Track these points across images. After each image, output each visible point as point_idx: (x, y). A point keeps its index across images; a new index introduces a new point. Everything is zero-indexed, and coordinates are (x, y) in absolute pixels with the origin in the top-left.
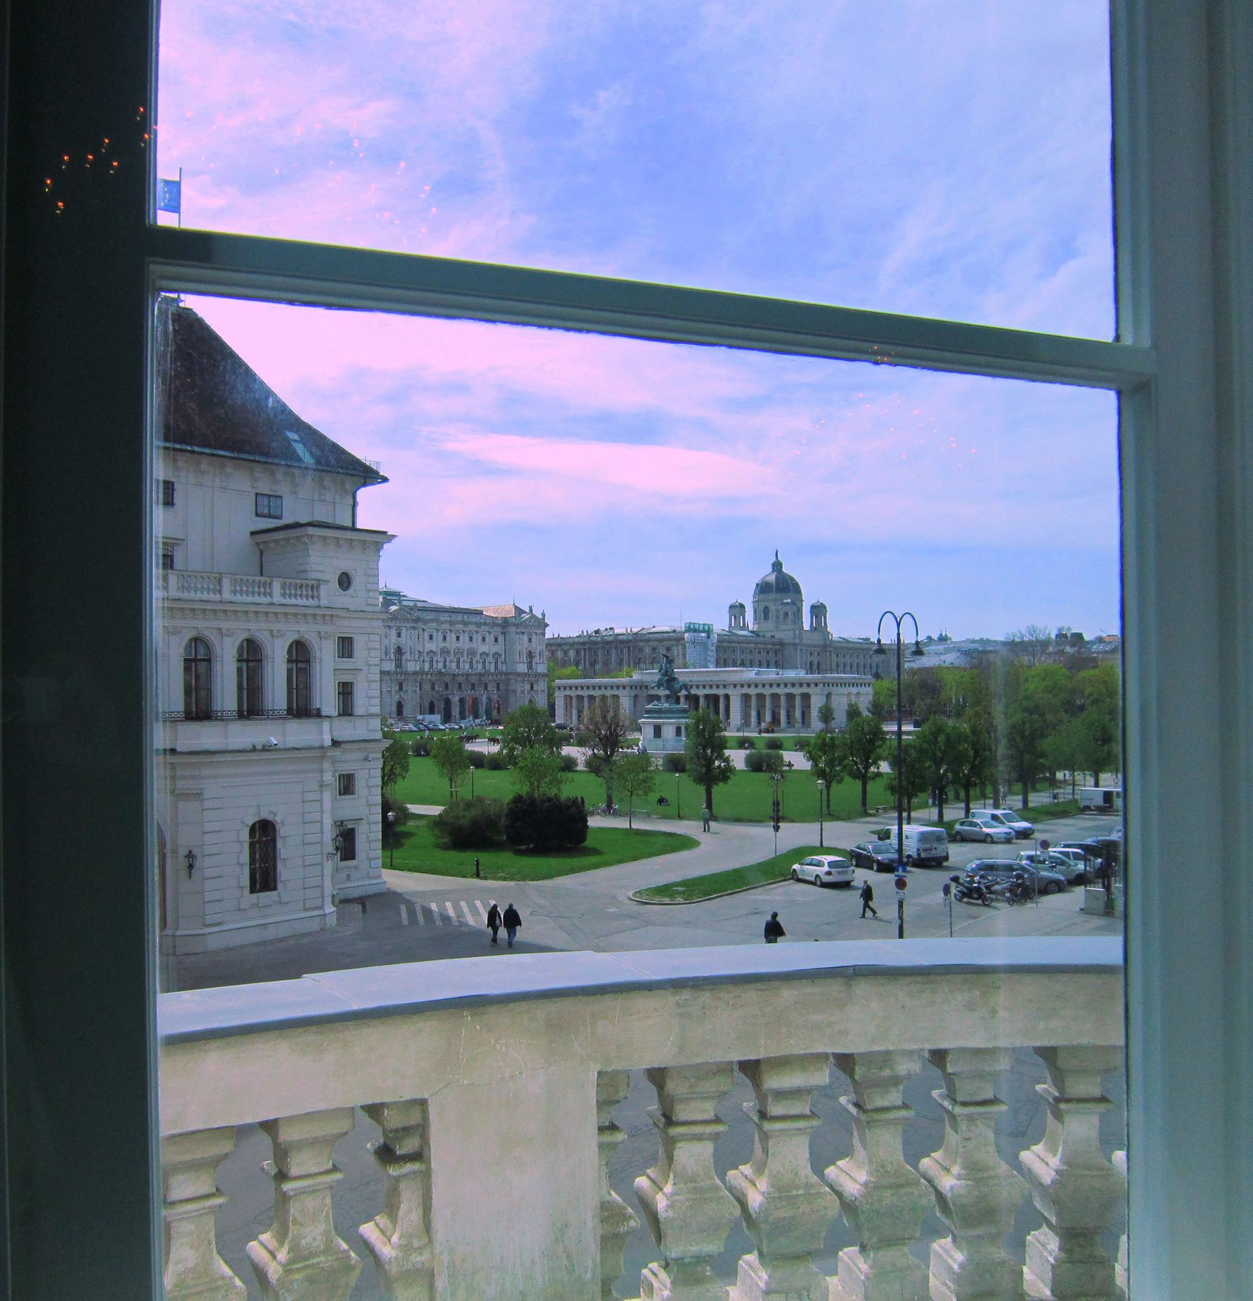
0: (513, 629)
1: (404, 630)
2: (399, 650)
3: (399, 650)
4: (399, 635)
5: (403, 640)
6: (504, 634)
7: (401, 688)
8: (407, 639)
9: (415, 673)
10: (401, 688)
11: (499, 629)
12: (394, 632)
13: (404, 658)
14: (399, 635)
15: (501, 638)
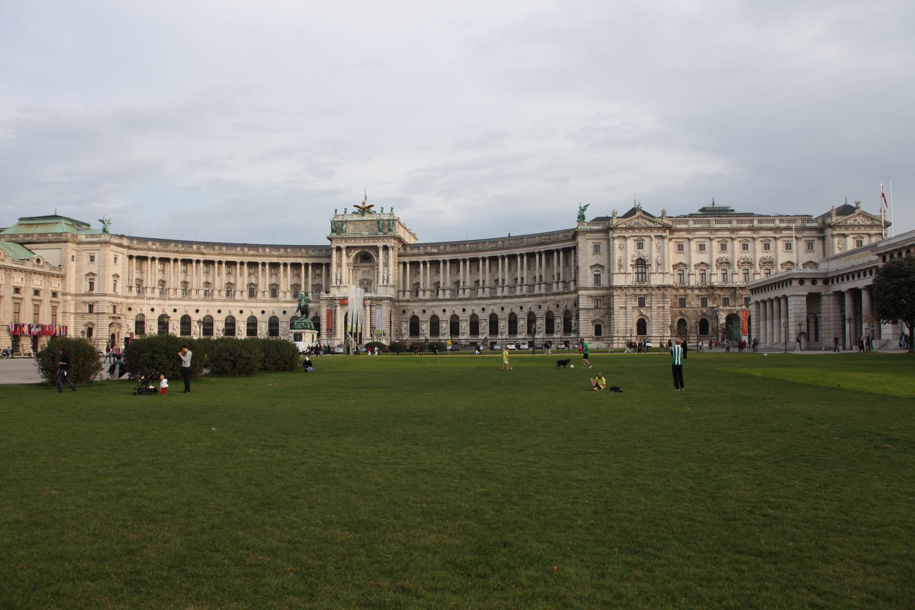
0: (829, 232)
1: (647, 240)
2: (641, 263)
3: (641, 263)
4: (640, 246)
5: (644, 253)
6: (823, 239)
7: (642, 303)
8: (652, 250)
9: (659, 287)
10: (642, 303)
11: (814, 233)
12: (631, 245)
13: (648, 271)
14: (640, 246)
15: (817, 244)
